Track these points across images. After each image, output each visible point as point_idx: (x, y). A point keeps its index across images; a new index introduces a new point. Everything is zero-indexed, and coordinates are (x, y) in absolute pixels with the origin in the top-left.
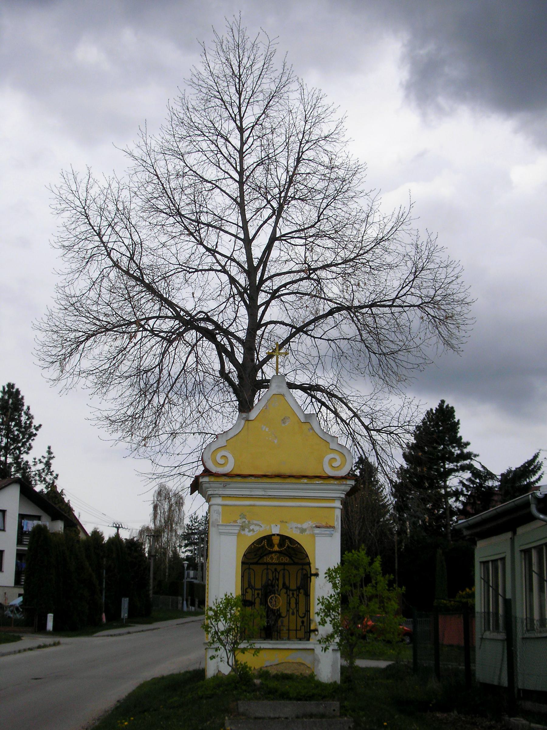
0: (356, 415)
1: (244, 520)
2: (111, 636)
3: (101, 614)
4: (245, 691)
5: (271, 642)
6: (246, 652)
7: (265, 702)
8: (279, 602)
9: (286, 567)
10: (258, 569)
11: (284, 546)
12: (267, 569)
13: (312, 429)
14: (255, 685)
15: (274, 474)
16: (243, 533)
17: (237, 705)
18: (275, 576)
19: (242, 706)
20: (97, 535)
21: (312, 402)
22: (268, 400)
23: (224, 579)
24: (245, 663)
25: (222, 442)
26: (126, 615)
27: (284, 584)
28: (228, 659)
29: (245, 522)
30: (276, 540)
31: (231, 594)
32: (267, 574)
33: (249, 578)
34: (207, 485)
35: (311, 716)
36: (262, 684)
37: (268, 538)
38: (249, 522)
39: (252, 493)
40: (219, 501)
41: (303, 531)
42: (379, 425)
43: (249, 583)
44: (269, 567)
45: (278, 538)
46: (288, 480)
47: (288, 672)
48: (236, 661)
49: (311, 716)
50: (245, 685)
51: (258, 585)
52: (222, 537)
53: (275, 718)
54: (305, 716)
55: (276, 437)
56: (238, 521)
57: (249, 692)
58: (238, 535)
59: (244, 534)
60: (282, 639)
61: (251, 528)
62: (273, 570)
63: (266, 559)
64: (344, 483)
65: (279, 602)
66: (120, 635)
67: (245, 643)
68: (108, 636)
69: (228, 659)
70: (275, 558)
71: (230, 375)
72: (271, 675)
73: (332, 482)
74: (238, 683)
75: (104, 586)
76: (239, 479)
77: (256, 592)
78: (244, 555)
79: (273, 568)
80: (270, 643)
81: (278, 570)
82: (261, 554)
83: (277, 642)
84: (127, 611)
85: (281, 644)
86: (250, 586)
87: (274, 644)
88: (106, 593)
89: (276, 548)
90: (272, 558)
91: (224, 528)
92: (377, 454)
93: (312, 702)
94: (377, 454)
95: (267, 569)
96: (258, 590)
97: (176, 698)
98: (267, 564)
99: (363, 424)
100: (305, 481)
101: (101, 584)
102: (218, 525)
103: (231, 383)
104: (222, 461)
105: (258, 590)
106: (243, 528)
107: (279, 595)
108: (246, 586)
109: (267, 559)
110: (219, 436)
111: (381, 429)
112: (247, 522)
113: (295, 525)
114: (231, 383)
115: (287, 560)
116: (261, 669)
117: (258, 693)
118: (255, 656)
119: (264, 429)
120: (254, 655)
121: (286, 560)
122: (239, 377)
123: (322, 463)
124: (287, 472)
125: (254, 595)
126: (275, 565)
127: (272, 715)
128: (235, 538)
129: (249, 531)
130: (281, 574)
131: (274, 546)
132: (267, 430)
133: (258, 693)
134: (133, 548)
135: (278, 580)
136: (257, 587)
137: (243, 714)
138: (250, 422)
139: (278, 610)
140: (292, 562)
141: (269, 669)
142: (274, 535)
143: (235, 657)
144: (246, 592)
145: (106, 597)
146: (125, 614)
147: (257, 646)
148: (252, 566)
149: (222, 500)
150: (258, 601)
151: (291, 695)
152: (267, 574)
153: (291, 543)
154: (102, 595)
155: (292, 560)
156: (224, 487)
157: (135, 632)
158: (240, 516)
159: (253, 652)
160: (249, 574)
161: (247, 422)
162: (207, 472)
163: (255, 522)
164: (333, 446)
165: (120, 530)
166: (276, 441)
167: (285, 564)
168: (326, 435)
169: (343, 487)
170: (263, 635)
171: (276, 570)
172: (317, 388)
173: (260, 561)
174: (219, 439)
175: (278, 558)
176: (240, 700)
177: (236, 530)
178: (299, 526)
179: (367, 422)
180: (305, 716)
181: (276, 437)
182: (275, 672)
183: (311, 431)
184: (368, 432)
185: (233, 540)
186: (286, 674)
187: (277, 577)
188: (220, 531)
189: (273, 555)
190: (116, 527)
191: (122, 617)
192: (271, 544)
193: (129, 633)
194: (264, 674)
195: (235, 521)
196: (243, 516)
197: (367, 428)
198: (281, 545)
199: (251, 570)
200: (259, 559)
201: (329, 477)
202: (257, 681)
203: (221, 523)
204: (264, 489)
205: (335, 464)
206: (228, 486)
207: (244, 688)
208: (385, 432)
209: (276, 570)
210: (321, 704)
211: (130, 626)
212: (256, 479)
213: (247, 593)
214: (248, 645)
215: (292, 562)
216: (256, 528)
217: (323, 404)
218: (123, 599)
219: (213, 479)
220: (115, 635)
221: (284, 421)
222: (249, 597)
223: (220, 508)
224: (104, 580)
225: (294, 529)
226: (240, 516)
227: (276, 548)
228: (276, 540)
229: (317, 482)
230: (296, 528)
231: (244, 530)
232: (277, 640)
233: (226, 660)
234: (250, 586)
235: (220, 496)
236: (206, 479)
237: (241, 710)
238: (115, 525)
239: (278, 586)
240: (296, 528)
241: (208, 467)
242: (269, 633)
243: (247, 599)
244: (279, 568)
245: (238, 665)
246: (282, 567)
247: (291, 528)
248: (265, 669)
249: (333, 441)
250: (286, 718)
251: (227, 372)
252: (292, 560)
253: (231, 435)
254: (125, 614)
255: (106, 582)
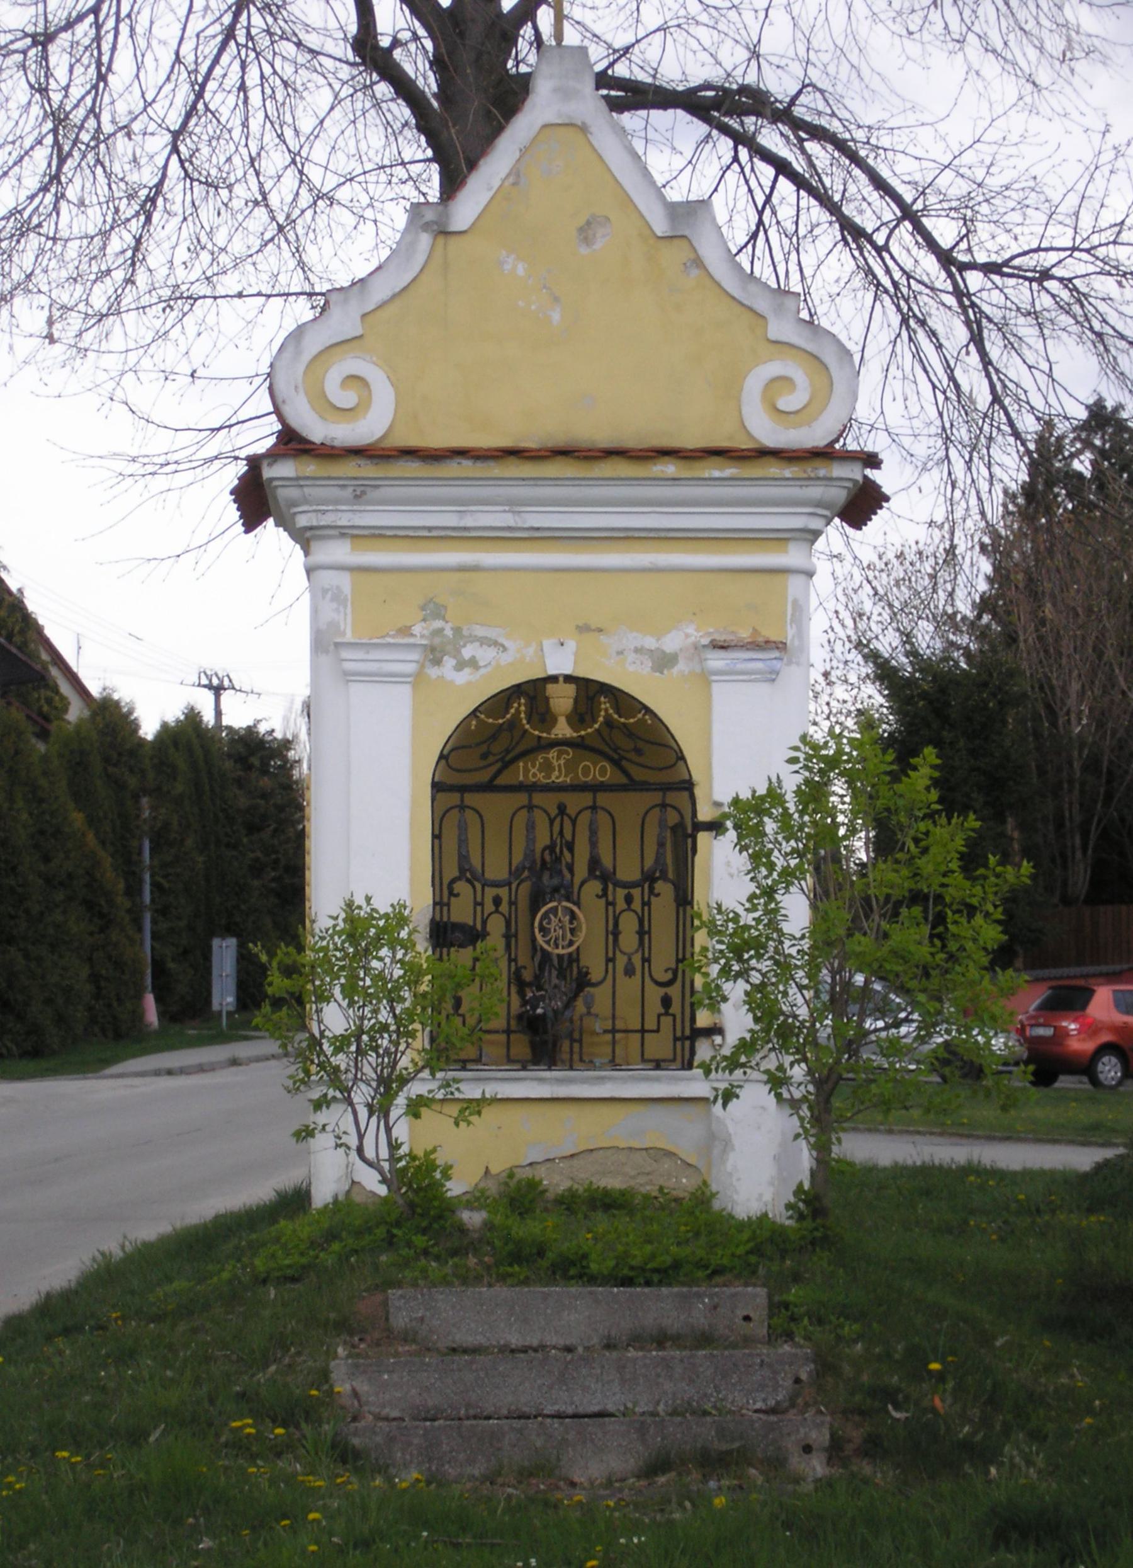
0: (908, 214)
1: (438, 624)
2: (170, 1072)
3: (139, 997)
4: (426, 1252)
5: (547, 1074)
6: (424, 1111)
7: (502, 1292)
8: (582, 928)
9: (603, 799)
10: (497, 807)
11: (595, 721)
12: (530, 807)
13: (698, 262)
14: (462, 1230)
15: (550, 444)
16: (433, 672)
17: (385, 1303)
18: (561, 833)
19: (404, 1307)
20: (111, 717)
21: (736, 159)
22: (524, 152)
23: (369, 850)
24: (427, 1154)
25: (344, 322)
26: (230, 999)
27: (594, 863)
28: (361, 1137)
29: (441, 631)
30: (562, 699)
31: (368, 899)
32: (531, 827)
33: (463, 842)
34: (292, 493)
35: (661, 1339)
36: (488, 1226)
37: (533, 692)
38: (457, 631)
39: (469, 522)
40: (338, 552)
41: (664, 662)
42: (988, 245)
43: (463, 857)
44: (538, 798)
45: (571, 690)
46: (607, 468)
47: (614, 1183)
48: (393, 1146)
49: (661, 1339)
50: (424, 1231)
51: (497, 869)
52: (354, 688)
53: (525, 1350)
54: (637, 1340)
55: (556, 299)
56: (417, 629)
57: (437, 1258)
58: (417, 680)
59: (441, 678)
60: (591, 1065)
61: (467, 653)
62: (554, 812)
63: (526, 771)
64: (822, 473)
65: (582, 928)
66: (201, 1069)
67: (423, 1080)
68: (157, 1073)
69: (361, 1137)
70: (557, 768)
71: (397, 54)
72: (550, 1195)
73: (774, 469)
74: (398, 1224)
75: (147, 898)
76: (413, 468)
77: (490, 892)
78: (442, 757)
79: (549, 802)
80: (541, 1080)
81: (572, 811)
82: (508, 751)
83: (522, 1074)
84: (231, 984)
85: (584, 1081)
86: (467, 873)
87: (559, 1081)
88: (154, 922)
89: (563, 730)
90: (547, 767)
91: (359, 654)
92: (986, 361)
93: (664, 1290)
94: (986, 361)
95: (530, 807)
96: (496, 884)
97: (178, 1285)
98: (531, 788)
99: (931, 244)
100: (670, 468)
101: (133, 891)
102: (337, 645)
103: (405, 89)
104: (347, 398)
105: (496, 884)
106: (434, 654)
107: (578, 904)
108: (452, 871)
109: (529, 771)
110: (333, 298)
111: (1006, 263)
112: (449, 633)
113: (633, 639)
114: (405, 89)
115: (603, 771)
116: (511, 1175)
117: (472, 1261)
118: (463, 1124)
119: (508, 267)
120: (457, 1124)
121: (599, 771)
122: (438, 63)
123: (739, 400)
124: (604, 438)
125: (482, 904)
126: (563, 788)
127: (515, 1340)
128: (403, 694)
129: (460, 666)
130: (584, 819)
131: (554, 721)
132: (521, 270)
133: (472, 1261)
134: (255, 761)
135: (571, 847)
136: (490, 875)
137: (407, 1337)
138: (453, 241)
139: (574, 958)
140: (624, 780)
141: (541, 1173)
142: (554, 679)
143: (388, 1130)
144: (451, 893)
145: (155, 936)
146: (224, 997)
147: (471, 1091)
148: (471, 799)
149: (353, 549)
150: (496, 926)
151: (594, 1267)
152: (531, 827)
153: (618, 712)
154: (140, 929)
155: (625, 772)
156: (358, 497)
157: (258, 1059)
158: (423, 608)
159: (454, 1110)
160: (463, 828)
161: (441, 240)
162: (290, 442)
163: (480, 631)
164: (780, 329)
165: (226, 696)
166: (556, 316)
167: (595, 788)
168: (753, 288)
169: (815, 492)
170: (521, 1046)
171: (562, 809)
172: (754, 101)
173: (501, 781)
174: (335, 312)
175: (570, 766)
176: (398, 1284)
177: (406, 663)
178: (650, 643)
179: (945, 231)
180: (637, 1340)
181: (556, 299)
182: (564, 1185)
183: (695, 272)
184: (950, 275)
185: (396, 704)
186: (606, 1192)
187: (568, 836)
188: (349, 666)
189: (553, 754)
190: (210, 687)
191: (215, 1007)
192: (542, 714)
193: (234, 1062)
194: (520, 1196)
195: (405, 631)
196: (433, 610)
197: (945, 258)
198: (578, 718)
199: (469, 814)
200: (499, 772)
201: (764, 453)
202: (473, 1219)
203: (349, 637)
204: (513, 504)
205: (790, 402)
206: (372, 494)
207: (420, 1241)
208: (1019, 274)
209: (562, 809)
210: (699, 1296)
211: (246, 1038)
212: (479, 464)
213: (457, 895)
214: (434, 1085)
215: (624, 780)
216: (485, 655)
217: (782, 168)
218: (216, 942)
219: (311, 468)
220: (183, 1071)
221: (586, 232)
222: (462, 912)
223: (344, 581)
224: (147, 877)
225: (631, 657)
226: (423, 608)
227: (563, 730)
228: (562, 699)
229: (717, 474)
230: (637, 650)
231: (438, 662)
232: (571, 1069)
233: (353, 1142)
234: (467, 873)
235: (343, 533)
236: (283, 470)
237: (400, 1320)
238: (204, 681)
239: (571, 868)
240: (637, 650)
241: (295, 423)
242: (543, 1038)
243: (455, 918)
244: (575, 802)
245: (400, 1159)
246: (586, 799)
247: (620, 653)
248: (527, 1173)
249: (779, 310)
250: (569, 1349)
251: (385, 42)
252: (625, 772)
253: (380, 292)
254: (224, 997)
255: (155, 885)
